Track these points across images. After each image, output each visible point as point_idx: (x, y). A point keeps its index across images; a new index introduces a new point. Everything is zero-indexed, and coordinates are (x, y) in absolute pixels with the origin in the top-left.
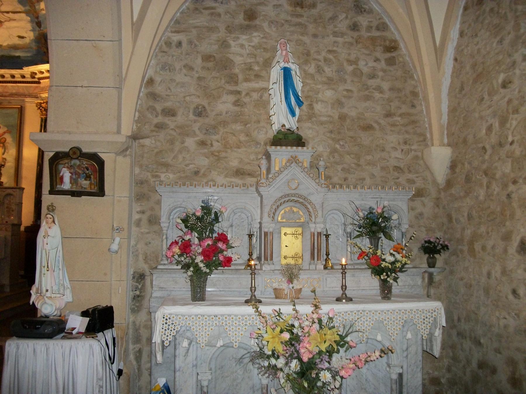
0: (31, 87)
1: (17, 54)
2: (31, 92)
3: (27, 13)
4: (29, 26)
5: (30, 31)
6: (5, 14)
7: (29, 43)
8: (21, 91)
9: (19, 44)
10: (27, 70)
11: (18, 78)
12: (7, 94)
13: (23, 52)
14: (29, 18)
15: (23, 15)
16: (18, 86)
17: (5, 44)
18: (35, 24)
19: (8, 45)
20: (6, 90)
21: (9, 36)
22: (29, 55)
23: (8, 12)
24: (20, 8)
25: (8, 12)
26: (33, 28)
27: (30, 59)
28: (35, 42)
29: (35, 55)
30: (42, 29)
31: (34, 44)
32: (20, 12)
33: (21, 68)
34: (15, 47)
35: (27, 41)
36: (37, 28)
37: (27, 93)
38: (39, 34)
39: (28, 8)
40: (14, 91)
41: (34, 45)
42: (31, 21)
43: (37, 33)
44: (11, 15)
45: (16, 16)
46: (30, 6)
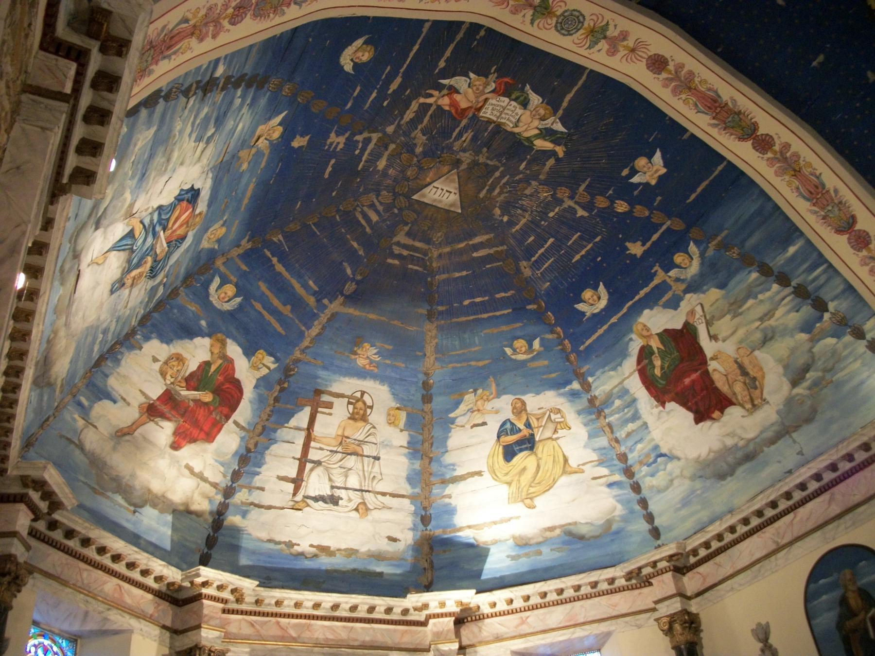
0: (395, 631)
1: (379, 570)
2: (397, 641)
3: (413, 498)
4: (409, 521)
5: (410, 529)
6: (379, 497)
7: (404, 552)
8: (380, 639)
9: (388, 552)
10: (413, 600)
11: (381, 613)
12: (356, 644)
13: (391, 565)
14: (413, 508)
15: (406, 502)
16: (374, 629)
17: (363, 549)
18: (418, 519)
19: (369, 550)
20: (352, 636)
21: (374, 536)
22: (398, 571)
23: (384, 494)
24: (406, 489)
25: (384, 494)
26: (414, 525)
27: (397, 578)
28: (413, 550)
29: (409, 572)
30: (429, 528)
31: (410, 552)
32: (403, 496)
33: (405, 597)
34: (379, 557)
35: (401, 546)
36: (421, 527)
37: (390, 643)
38: (421, 537)
39: (418, 490)
40: (367, 639)
41: (409, 557)
42: (415, 513)
43: (419, 533)
44: (387, 500)
45: (395, 502)
46: (422, 489)
